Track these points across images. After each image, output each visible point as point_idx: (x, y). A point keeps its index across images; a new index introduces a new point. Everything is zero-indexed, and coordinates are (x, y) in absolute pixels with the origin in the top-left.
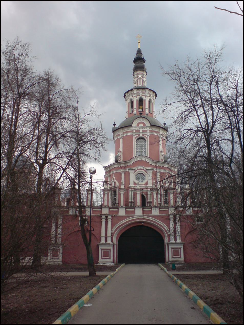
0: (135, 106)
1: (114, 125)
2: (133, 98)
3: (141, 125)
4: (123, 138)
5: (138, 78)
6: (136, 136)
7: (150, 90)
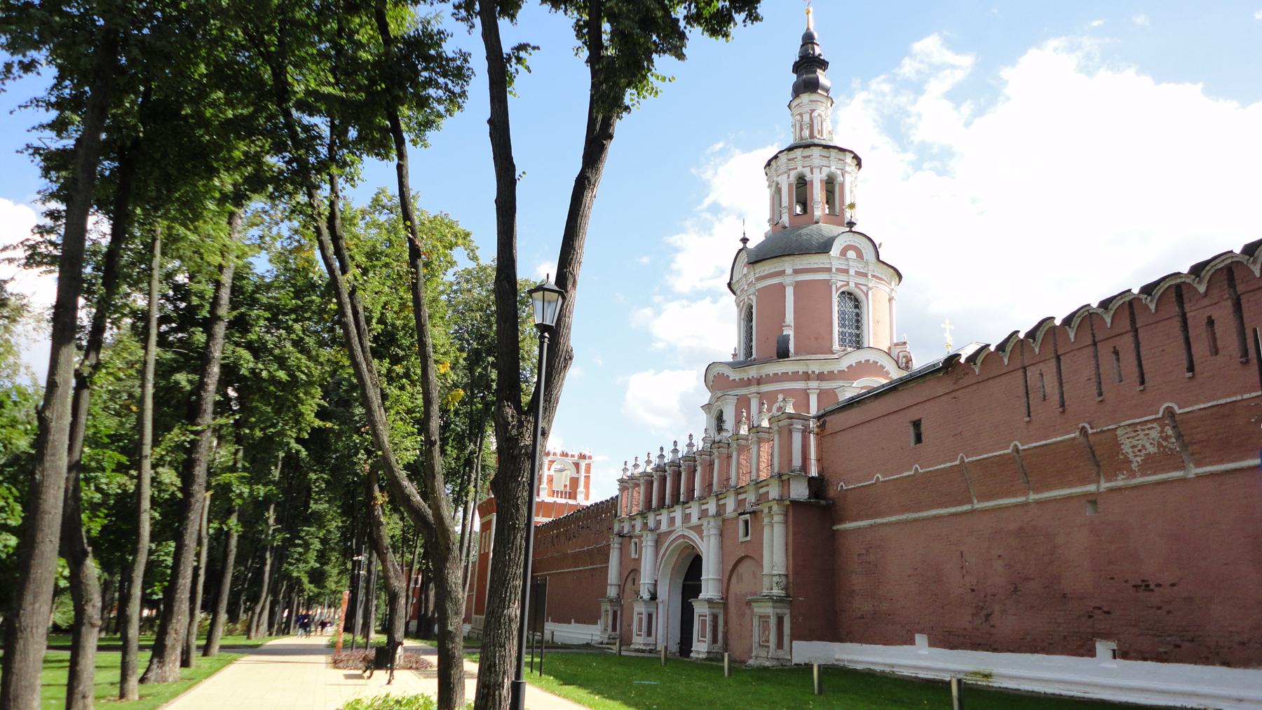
0: (818, 193)
1: (745, 240)
2: (807, 171)
3: (851, 254)
4: (798, 286)
5: (815, 114)
6: (839, 284)
7: (856, 157)
